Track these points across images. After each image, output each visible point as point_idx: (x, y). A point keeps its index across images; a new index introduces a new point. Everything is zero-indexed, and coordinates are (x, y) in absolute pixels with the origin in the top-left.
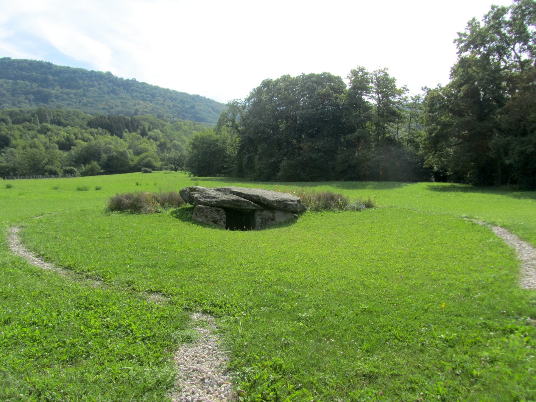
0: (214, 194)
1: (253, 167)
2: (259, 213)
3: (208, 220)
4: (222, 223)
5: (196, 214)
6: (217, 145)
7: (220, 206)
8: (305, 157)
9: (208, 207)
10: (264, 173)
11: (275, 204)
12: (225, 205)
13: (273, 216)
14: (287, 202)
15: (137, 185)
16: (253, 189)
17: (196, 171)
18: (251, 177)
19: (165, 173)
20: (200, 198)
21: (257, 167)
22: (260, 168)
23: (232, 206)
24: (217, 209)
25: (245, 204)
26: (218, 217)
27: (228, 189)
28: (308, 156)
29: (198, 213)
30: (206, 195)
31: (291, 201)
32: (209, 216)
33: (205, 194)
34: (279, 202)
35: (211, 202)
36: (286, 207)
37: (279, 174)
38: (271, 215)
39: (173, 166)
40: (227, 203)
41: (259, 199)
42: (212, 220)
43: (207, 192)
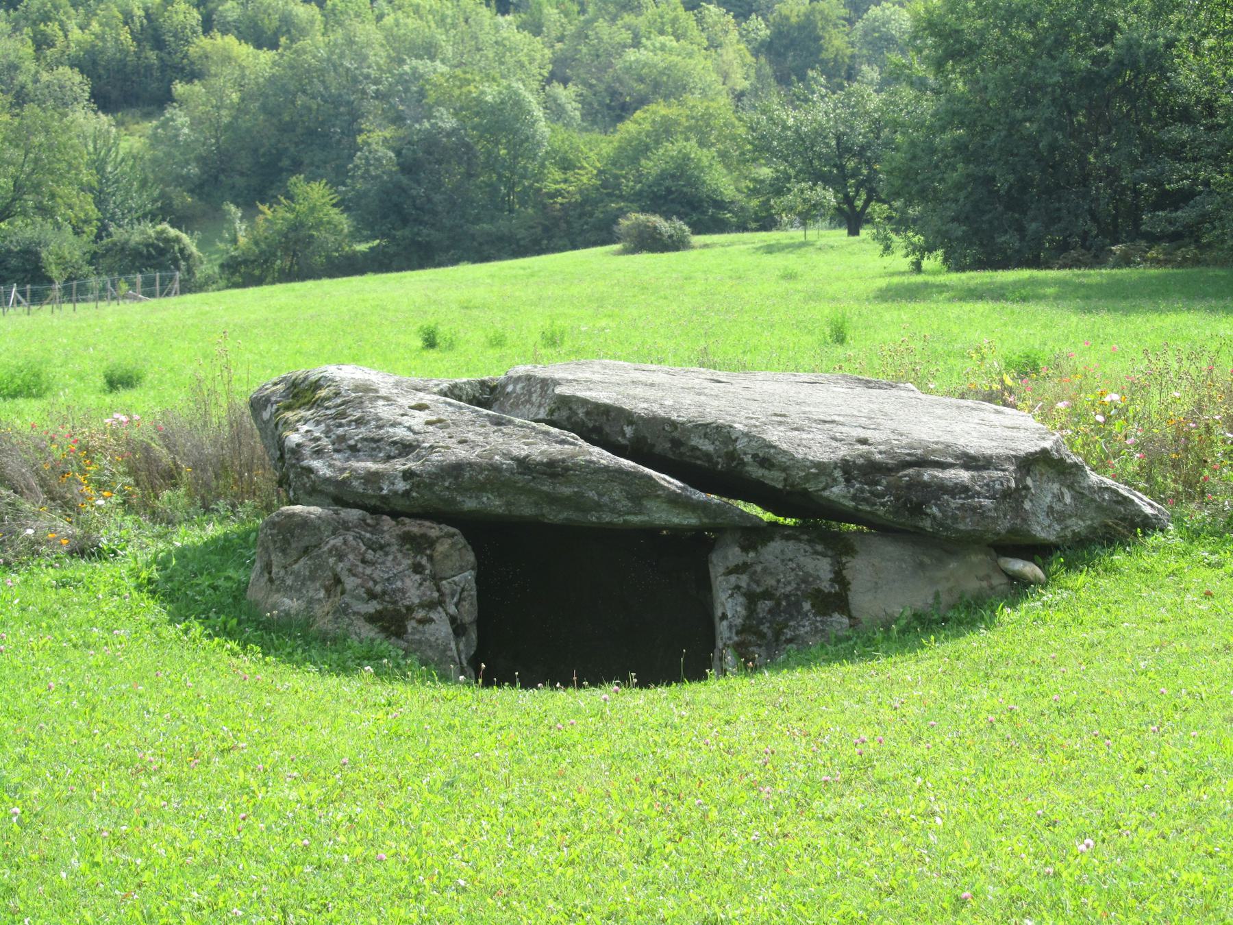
0: (418, 420)
2: (735, 555)
3: (343, 611)
4: (441, 628)
5: (268, 567)
6: (1113, 27)
7: (437, 505)
9: (354, 514)
11: (837, 492)
12: (470, 504)
13: (839, 578)
14: (927, 474)
15: (430, 342)
17: (959, 230)
19: (770, 249)
20: (318, 453)
23: (526, 509)
26: (413, 590)
31: (971, 462)
32: (350, 582)
34: (864, 470)
35: (372, 478)
36: (917, 510)
38: (822, 568)
39: (830, 197)
40: (481, 487)
41: (732, 456)
42: (373, 607)
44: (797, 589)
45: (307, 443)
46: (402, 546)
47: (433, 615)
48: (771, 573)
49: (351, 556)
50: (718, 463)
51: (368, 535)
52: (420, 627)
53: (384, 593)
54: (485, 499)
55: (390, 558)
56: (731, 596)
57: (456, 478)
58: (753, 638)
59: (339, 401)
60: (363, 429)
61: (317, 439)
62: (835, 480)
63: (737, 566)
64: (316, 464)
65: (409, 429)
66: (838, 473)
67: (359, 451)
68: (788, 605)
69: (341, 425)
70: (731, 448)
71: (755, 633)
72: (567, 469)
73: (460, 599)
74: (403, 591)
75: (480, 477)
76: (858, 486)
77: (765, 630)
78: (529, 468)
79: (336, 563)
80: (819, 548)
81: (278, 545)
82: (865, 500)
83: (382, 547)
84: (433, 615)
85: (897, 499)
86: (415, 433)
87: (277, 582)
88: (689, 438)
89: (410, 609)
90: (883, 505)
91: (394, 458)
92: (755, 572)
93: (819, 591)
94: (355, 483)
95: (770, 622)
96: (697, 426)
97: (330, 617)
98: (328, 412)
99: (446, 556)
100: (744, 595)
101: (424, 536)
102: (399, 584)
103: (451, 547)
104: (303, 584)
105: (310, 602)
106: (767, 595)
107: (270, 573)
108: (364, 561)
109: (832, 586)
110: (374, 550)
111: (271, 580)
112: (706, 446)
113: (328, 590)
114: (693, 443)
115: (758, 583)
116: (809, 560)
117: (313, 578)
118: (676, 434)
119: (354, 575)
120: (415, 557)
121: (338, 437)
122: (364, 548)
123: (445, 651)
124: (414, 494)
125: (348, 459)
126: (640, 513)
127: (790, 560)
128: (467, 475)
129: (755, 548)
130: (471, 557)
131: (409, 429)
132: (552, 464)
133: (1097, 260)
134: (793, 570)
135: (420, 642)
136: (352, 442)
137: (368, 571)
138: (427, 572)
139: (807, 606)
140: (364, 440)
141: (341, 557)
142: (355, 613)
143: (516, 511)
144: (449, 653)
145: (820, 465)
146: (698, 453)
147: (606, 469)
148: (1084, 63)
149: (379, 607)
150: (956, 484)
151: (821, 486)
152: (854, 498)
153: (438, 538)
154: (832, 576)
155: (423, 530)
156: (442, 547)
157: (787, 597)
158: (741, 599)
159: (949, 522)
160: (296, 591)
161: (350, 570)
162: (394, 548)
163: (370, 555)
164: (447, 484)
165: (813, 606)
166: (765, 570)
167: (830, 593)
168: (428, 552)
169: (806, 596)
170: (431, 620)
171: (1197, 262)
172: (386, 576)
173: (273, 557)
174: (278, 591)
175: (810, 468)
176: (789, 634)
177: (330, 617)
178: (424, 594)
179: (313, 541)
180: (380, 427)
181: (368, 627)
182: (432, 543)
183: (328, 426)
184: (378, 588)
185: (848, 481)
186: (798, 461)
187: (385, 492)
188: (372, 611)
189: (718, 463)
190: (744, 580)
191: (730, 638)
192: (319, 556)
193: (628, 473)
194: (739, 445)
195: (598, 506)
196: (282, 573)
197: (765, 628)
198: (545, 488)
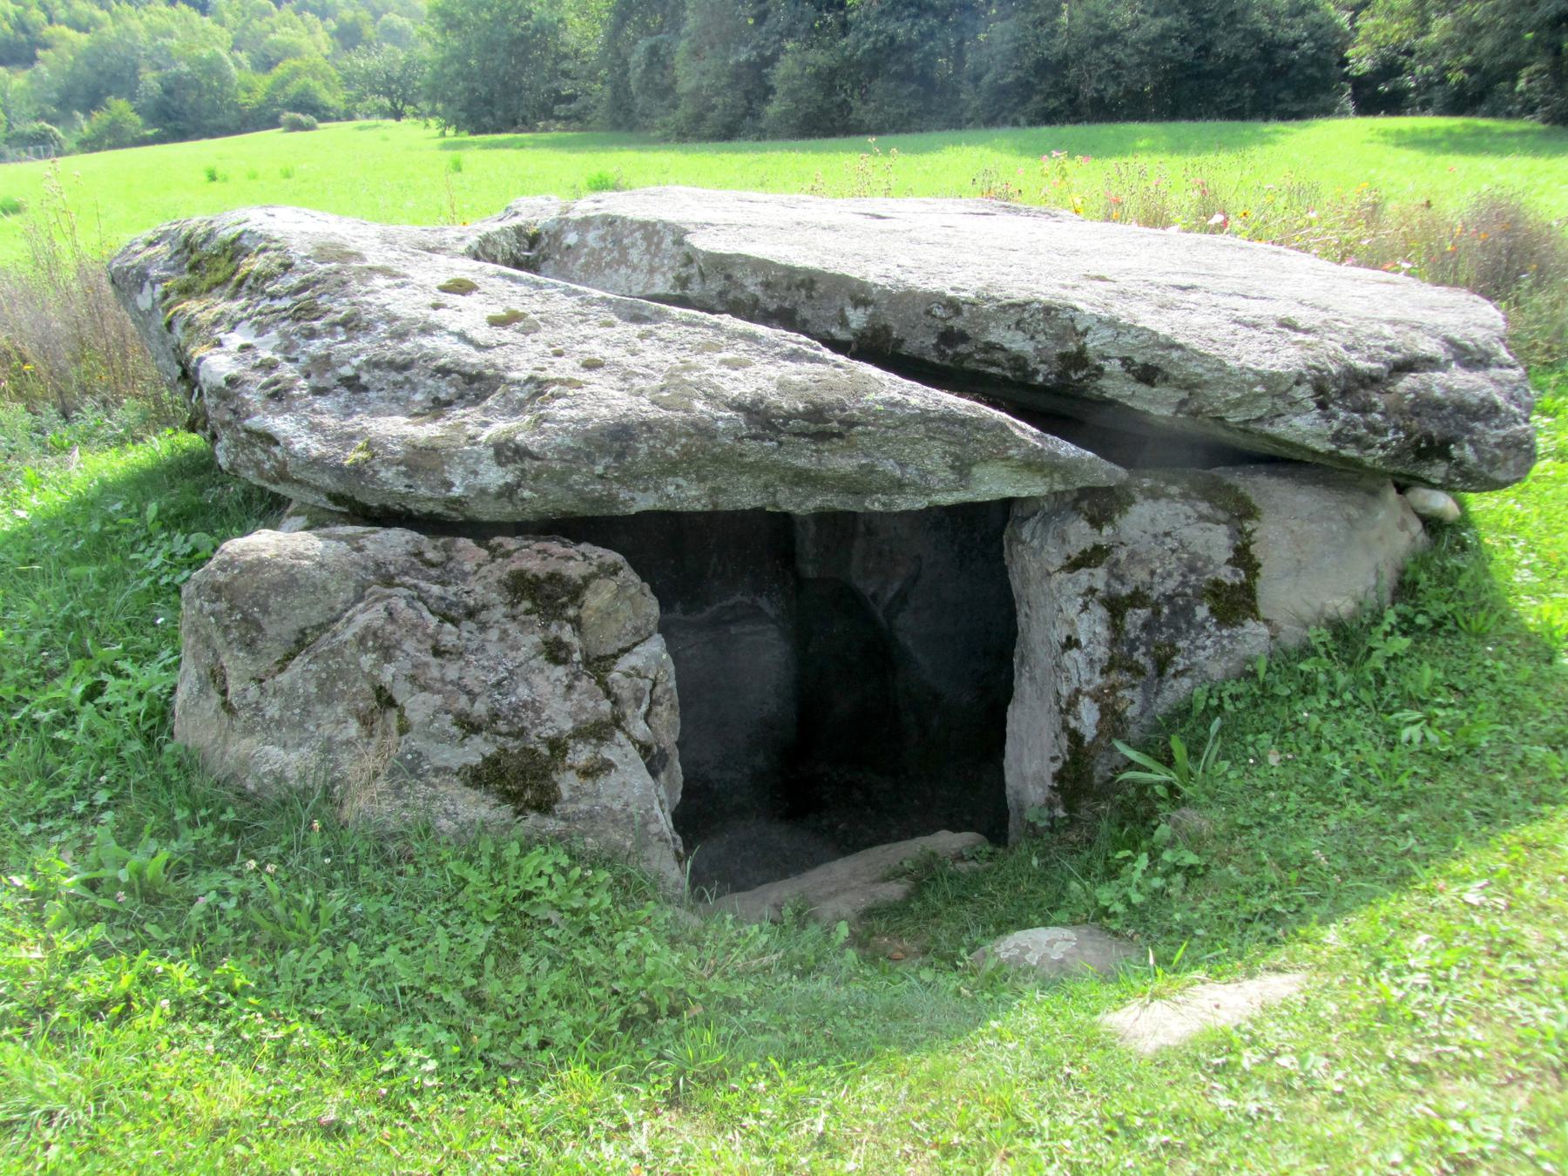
0: (470, 314)
1: (669, 90)
2: (1081, 535)
3: (412, 768)
5: (216, 677)
6: (530, 12)
8: (867, 35)
9: (394, 542)
10: (714, 107)
12: (645, 502)
13: (1243, 558)
15: (213, 178)
16: (906, 211)
17: (463, 115)
18: (665, 125)
19: (361, 128)
20: (279, 396)
21: (685, 85)
22: (699, 88)
23: (745, 496)
24: (532, 558)
25: (935, 459)
26: (556, 701)
27: (650, 231)
28: (879, 33)
29: (237, 666)
30: (355, 352)
32: (418, 707)
33: (352, 325)
34: (1342, 389)
35: (421, 459)
37: (773, 109)
39: (387, 103)
41: (1078, 360)
42: (477, 750)
43: (384, 296)
44: (1184, 584)
45: (250, 376)
46: (513, 605)
47: (608, 753)
48: (1141, 561)
49: (409, 645)
50: (1036, 372)
51: (436, 589)
52: (588, 785)
53: (495, 716)
54: (671, 489)
55: (493, 634)
56: (1085, 607)
57: (620, 456)
58: (1126, 677)
59: (295, 280)
60: (363, 343)
61: (269, 366)
62: (1293, 403)
63: (1084, 552)
64: (280, 424)
65: (462, 336)
66: (1304, 393)
67: (366, 389)
68: (1173, 613)
69: (312, 334)
70: (1072, 347)
71: (1129, 669)
72: (851, 423)
73: (653, 703)
74: (534, 706)
75: (670, 451)
76: (1342, 415)
77: (1142, 660)
78: (773, 427)
80: (1204, 507)
81: (234, 634)
82: (1357, 440)
83: (471, 614)
84: (608, 753)
85: (1408, 437)
86: (479, 347)
87: (245, 714)
88: (985, 330)
89: (557, 746)
90: (1383, 447)
91: (449, 403)
92: (1118, 561)
93: (1217, 583)
94: (386, 474)
95: (1147, 644)
96: (1004, 309)
97: (381, 784)
98: (278, 304)
99: (607, 614)
100: (1103, 602)
101: (553, 577)
102: (523, 692)
103: (618, 600)
104: (306, 712)
105: (328, 747)
106: (1137, 599)
107: (224, 693)
108: (437, 652)
109: (1235, 574)
110: (455, 622)
111: (227, 706)
112: (1018, 343)
113: (366, 721)
114: (992, 338)
115: (1121, 579)
116: (1197, 533)
118: (957, 323)
119: (424, 688)
120: (546, 627)
121: (314, 360)
122: (433, 621)
123: (645, 825)
124: (526, 494)
125: (348, 412)
126: (966, 488)
127: (1167, 534)
128: (643, 448)
129: (1110, 520)
130: (652, 607)
131: (462, 336)
132: (816, 413)
133: (532, 129)
134: (1173, 551)
135: (591, 816)
136: (347, 371)
137: (452, 672)
138: (577, 657)
139: (1202, 612)
140: (374, 364)
141: (387, 652)
142: (438, 771)
143: (725, 503)
144: (653, 828)
145: (1271, 381)
146: (998, 356)
147: (924, 417)
148: (518, 31)
149: (490, 750)
150: (1483, 400)
151: (1258, 413)
152: (1337, 437)
153: (587, 580)
154: (1231, 554)
155: (552, 566)
156: (598, 598)
157: (1169, 599)
158: (1101, 612)
159: (1485, 469)
160: (294, 726)
161: (413, 679)
162: (498, 613)
163: (449, 636)
164: (599, 469)
165: (1212, 610)
166: (1132, 556)
167: (1233, 586)
168: (571, 612)
169: (1200, 596)
170: (608, 766)
171: (581, 130)
172: (493, 678)
173: (225, 659)
174: (249, 731)
175: (1252, 385)
176: (1180, 662)
177: (381, 784)
178: (582, 709)
179: (316, 616)
180: (401, 336)
181: (473, 795)
182: (576, 592)
183: (285, 335)
184: (480, 709)
185: (1322, 405)
186: (1230, 374)
187: (457, 491)
188: (476, 760)
189: (1036, 372)
190: (1098, 577)
191: (1089, 682)
192: (334, 652)
193: (964, 422)
194: (1092, 343)
195: (900, 486)
196: (253, 692)
197: (1140, 656)
198: (801, 463)
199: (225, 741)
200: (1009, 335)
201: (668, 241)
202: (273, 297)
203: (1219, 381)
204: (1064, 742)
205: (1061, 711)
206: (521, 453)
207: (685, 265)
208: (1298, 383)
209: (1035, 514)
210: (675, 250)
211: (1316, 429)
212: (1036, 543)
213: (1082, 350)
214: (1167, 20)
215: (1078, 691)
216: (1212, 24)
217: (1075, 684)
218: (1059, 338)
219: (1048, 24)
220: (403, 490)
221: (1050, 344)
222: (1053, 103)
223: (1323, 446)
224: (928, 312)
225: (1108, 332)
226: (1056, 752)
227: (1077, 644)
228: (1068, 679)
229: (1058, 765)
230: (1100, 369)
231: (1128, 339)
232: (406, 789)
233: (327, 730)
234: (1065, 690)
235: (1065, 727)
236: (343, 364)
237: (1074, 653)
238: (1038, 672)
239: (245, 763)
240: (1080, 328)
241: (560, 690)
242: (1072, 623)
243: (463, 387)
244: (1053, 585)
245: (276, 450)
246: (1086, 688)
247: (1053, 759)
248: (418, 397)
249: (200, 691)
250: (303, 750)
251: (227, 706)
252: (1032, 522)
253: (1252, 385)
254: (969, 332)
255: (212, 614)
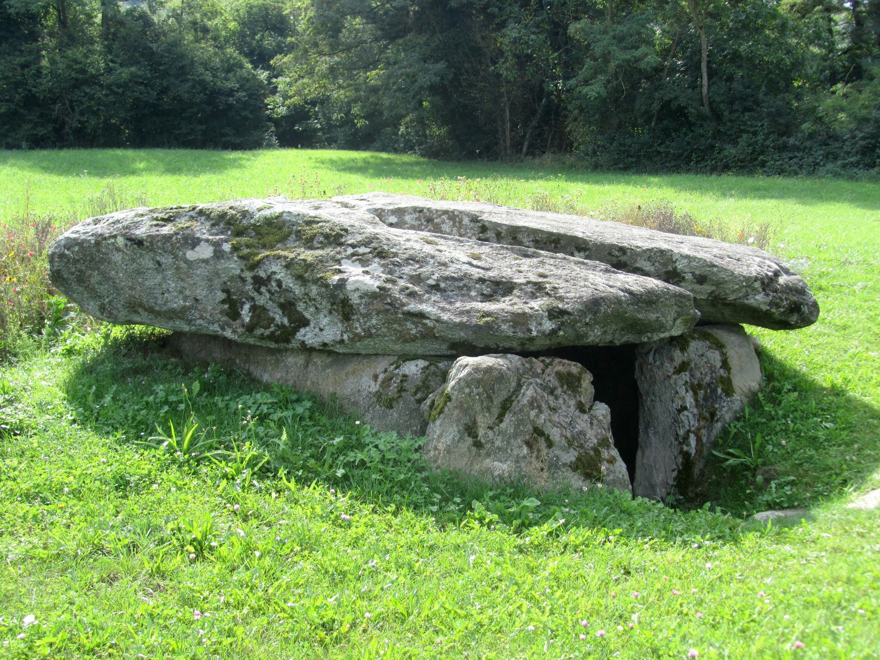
5: (470, 430)
29: (483, 421)
44: (712, 378)
57: (595, 313)
62: (754, 289)
66: (757, 285)
70: (670, 268)
74: (582, 433)
79: (537, 416)
88: (636, 261)
94: (504, 327)
106: (700, 386)
111: (478, 445)
114: (638, 265)
117: (515, 435)
118: (624, 258)
136: (431, 282)
145: (747, 279)
174: (488, 455)
175: (742, 282)
187: (534, 333)
194: (679, 266)
199: (472, 464)
200: (645, 263)
201: (466, 221)
202: (353, 246)
203: (730, 281)
204: (680, 460)
205: (680, 443)
206: (563, 312)
207: (482, 232)
208: (755, 281)
209: (651, 350)
210: (472, 225)
211: (764, 300)
212: (658, 363)
213: (675, 269)
214: (133, 69)
215: (689, 431)
216: (165, 74)
217: (687, 427)
218: (665, 265)
219: (33, 67)
220: (512, 334)
221: (661, 267)
222: (41, 131)
223: (765, 308)
224: (610, 254)
225: (686, 261)
226: (674, 466)
227: (685, 408)
228: (684, 426)
229: (675, 474)
230: (684, 278)
231: (694, 263)
232: (555, 475)
233: (515, 452)
234: (681, 432)
235: (681, 451)
236: (428, 278)
237: (686, 413)
238: (660, 429)
239: (483, 473)
240: (674, 259)
241: (589, 425)
242: (683, 399)
243: (493, 287)
244: (672, 381)
245: (427, 321)
246: (693, 429)
247: (673, 470)
248: (473, 293)
249: (460, 438)
250: (509, 463)
251: (478, 445)
252: (652, 353)
253: (742, 282)
254: (628, 263)
255: (478, 394)
